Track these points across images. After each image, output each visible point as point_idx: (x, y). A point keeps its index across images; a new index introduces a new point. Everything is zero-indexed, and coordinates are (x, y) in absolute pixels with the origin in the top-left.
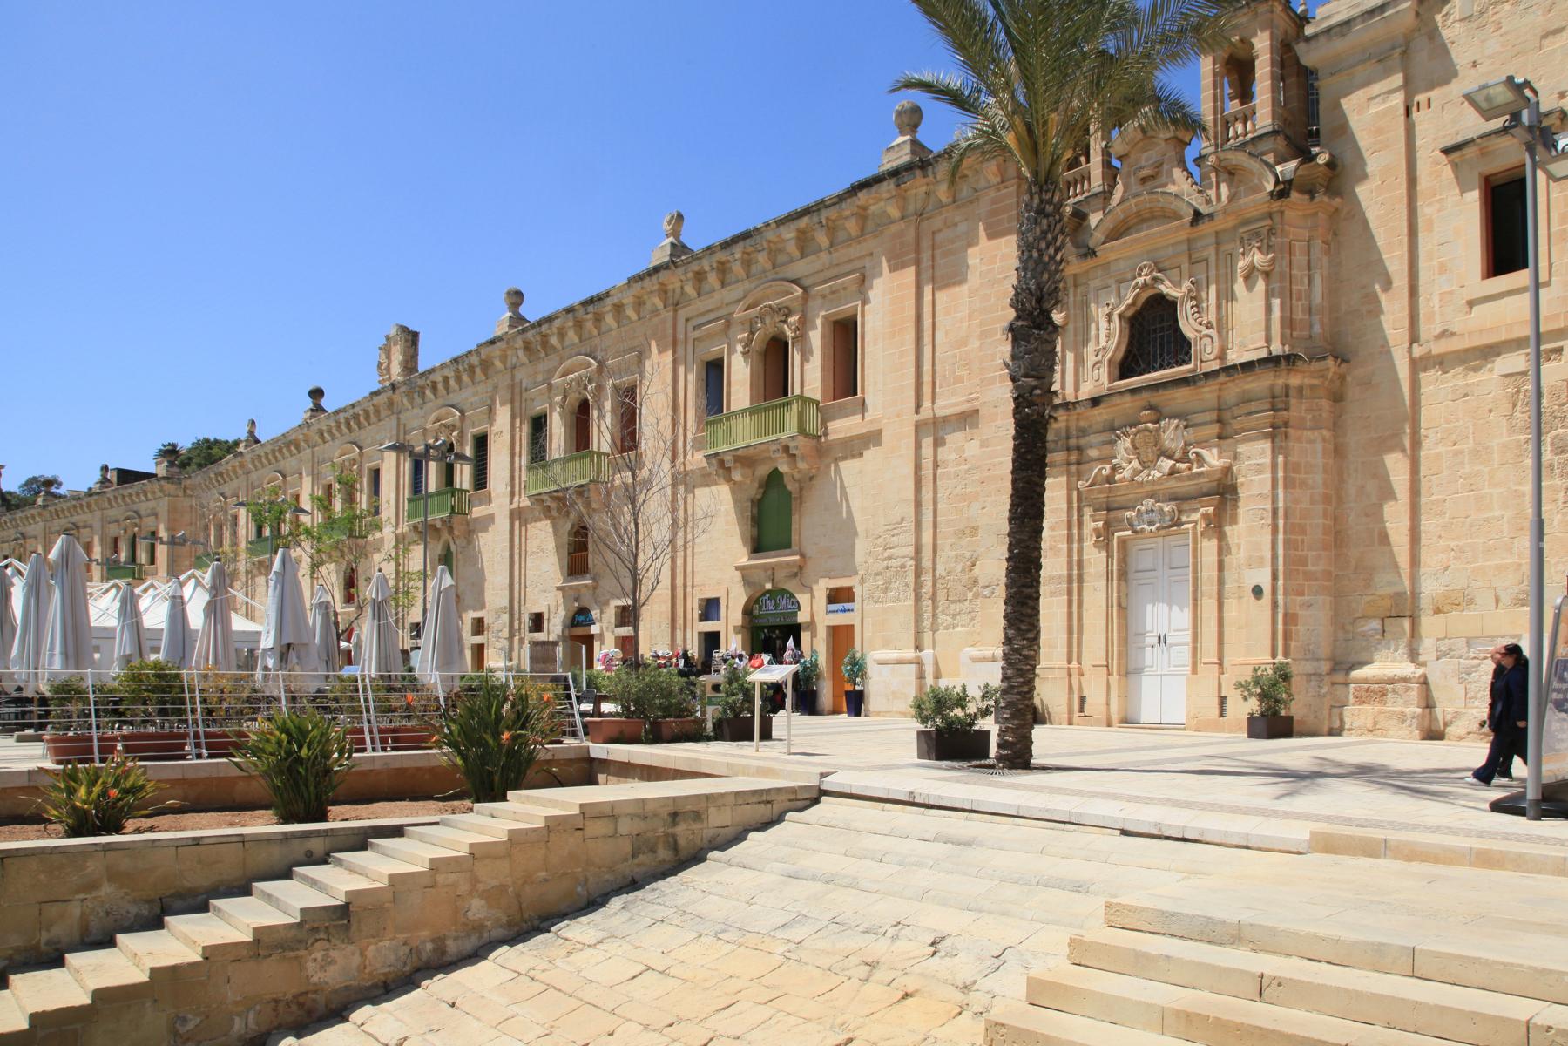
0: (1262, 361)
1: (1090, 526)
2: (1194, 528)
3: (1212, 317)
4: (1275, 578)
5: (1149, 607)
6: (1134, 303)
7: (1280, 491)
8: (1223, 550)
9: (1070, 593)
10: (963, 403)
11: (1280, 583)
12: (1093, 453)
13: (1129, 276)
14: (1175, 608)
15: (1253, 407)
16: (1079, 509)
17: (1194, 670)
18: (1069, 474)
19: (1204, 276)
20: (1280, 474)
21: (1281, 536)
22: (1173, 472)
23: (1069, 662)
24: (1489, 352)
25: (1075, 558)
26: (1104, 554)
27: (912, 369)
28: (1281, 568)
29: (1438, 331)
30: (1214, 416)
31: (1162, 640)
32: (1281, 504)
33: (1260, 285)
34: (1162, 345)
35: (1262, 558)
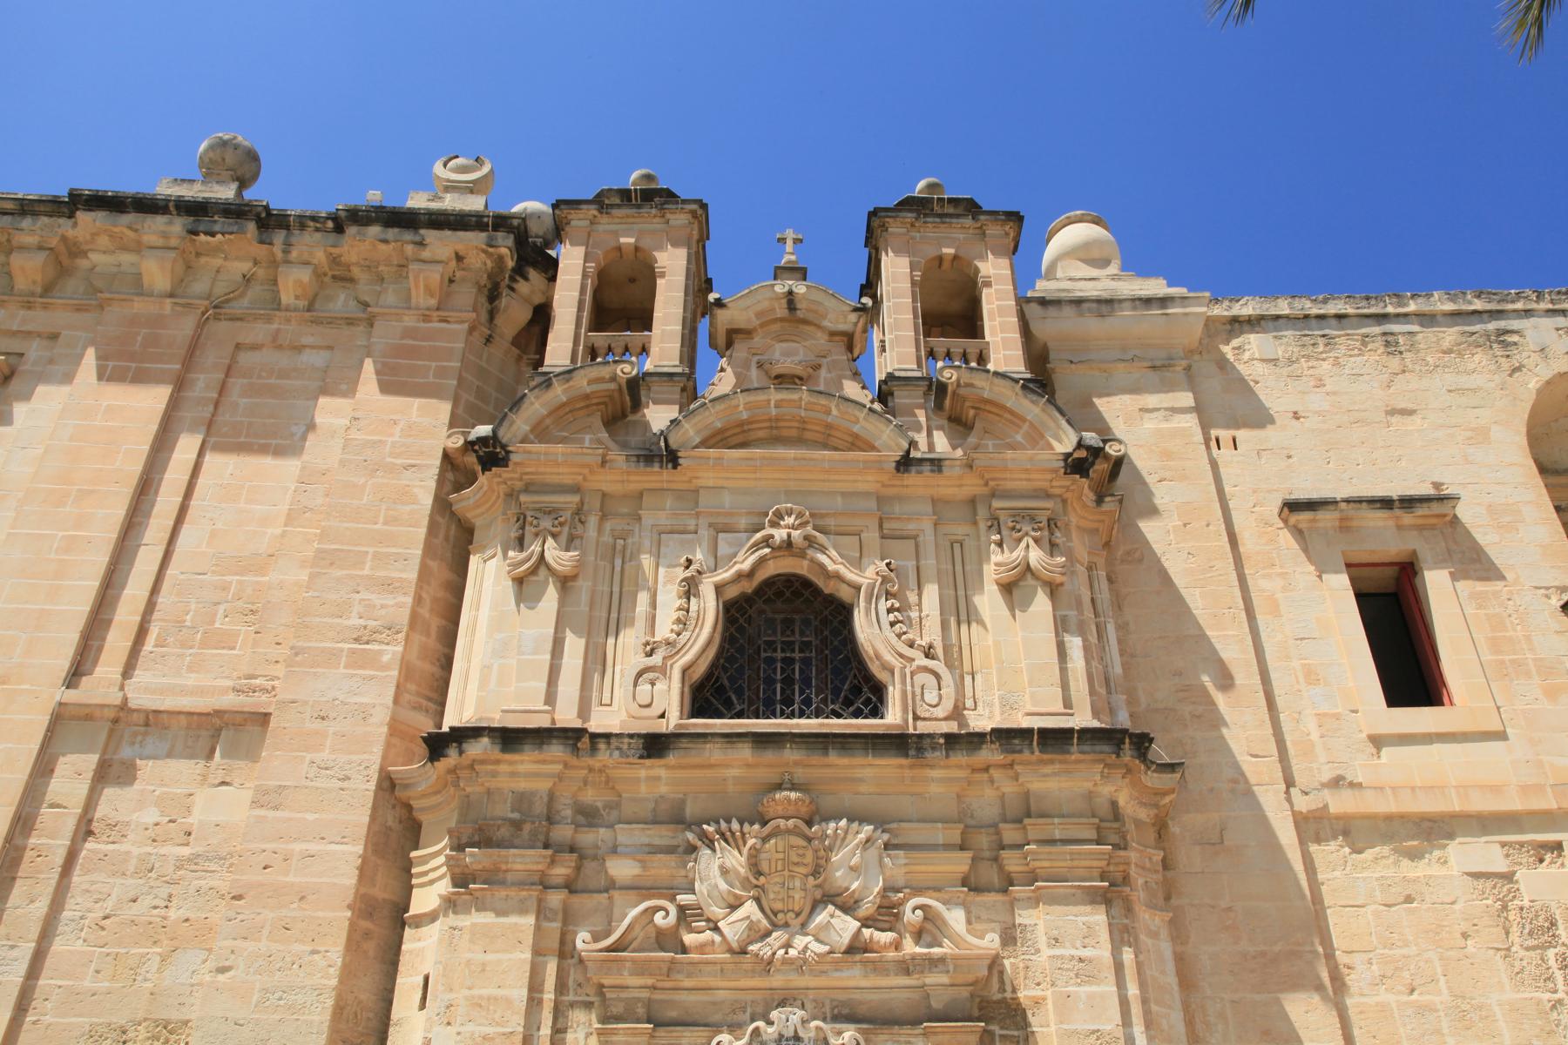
3: (931, 634)
6: (751, 574)
10: (224, 691)
12: (622, 869)
13: (743, 522)
16: (558, 1012)
18: (541, 912)
19: (911, 564)
22: (856, 948)
24: (1429, 830)
27: (91, 585)
29: (1326, 776)
30: (955, 835)
33: (1042, 603)
34: (788, 681)
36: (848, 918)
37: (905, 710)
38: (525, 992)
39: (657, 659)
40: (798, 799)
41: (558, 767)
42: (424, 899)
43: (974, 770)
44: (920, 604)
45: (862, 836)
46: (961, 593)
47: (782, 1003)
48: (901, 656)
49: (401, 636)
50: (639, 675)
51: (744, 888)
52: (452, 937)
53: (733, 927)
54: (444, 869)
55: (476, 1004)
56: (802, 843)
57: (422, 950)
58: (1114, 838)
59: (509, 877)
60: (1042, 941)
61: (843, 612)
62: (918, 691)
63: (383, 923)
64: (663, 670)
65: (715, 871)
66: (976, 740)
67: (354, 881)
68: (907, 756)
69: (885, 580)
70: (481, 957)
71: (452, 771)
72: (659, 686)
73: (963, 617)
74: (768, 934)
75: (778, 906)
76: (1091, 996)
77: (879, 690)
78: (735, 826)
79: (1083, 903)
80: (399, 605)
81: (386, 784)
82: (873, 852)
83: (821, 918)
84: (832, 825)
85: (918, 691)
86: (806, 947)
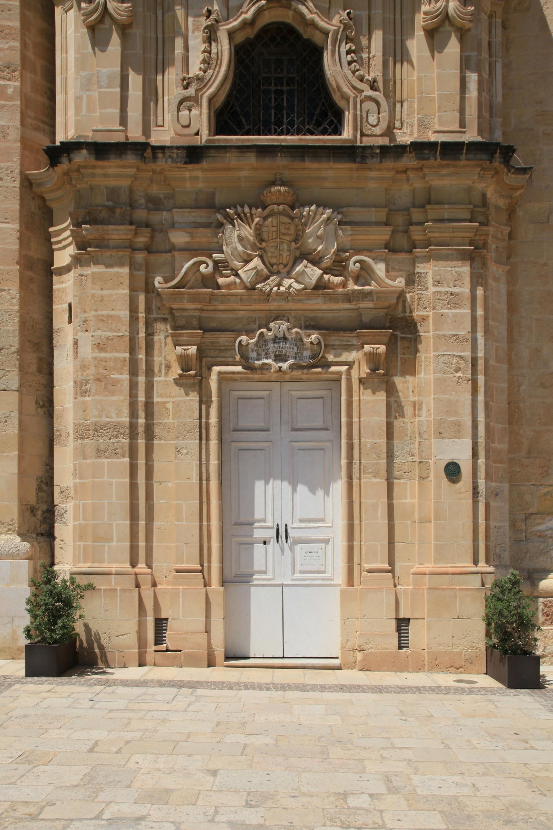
0: (473, 147)
1: (168, 352)
2: (348, 373)
3: (375, 72)
4: (475, 455)
5: (259, 485)
6: (251, 23)
7: (480, 335)
8: (394, 409)
9: (133, 454)
11: (481, 461)
12: (179, 238)
14: (302, 489)
15: (446, 212)
16: (148, 324)
17: (350, 582)
18: (133, 266)
19: (364, 14)
20: (480, 312)
21: (481, 398)
22: (320, 286)
23: (133, 564)
25: (142, 398)
26: (194, 397)
28: (481, 440)
30: (382, 215)
31: (281, 534)
32: (481, 354)
33: (453, 47)
35: (458, 424)
36: (316, 268)
37: (355, 129)
38: (127, 313)
39: (191, 91)
40: (285, 192)
41: (132, 171)
42: (62, 258)
43: (397, 172)
44: (369, 47)
45: (325, 216)
46: (398, 38)
47: (276, 319)
48: (355, 88)
49: (17, 73)
50: (181, 103)
51: (253, 250)
52: (81, 281)
53: (246, 273)
54: (71, 239)
55: (101, 319)
56: (288, 221)
57: (65, 288)
58: (481, 218)
59: (111, 243)
60: (430, 282)
61: (316, 53)
62: (364, 115)
63: (39, 275)
64: (195, 100)
65: (235, 239)
66: (400, 150)
67: (17, 247)
68: (355, 162)
69: (346, 27)
70: (99, 292)
71: (66, 173)
72: (195, 112)
73: (398, 58)
74: (268, 278)
75: (274, 261)
76: (455, 315)
77: (339, 115)
78: (247, 210)
79: (457, 260)
80: (12, 49)
81: (26, 183)
82: (331, 227)
83: (299, 268)
84: (307, 209)
85: (364, 115)
86: (290, 286)
